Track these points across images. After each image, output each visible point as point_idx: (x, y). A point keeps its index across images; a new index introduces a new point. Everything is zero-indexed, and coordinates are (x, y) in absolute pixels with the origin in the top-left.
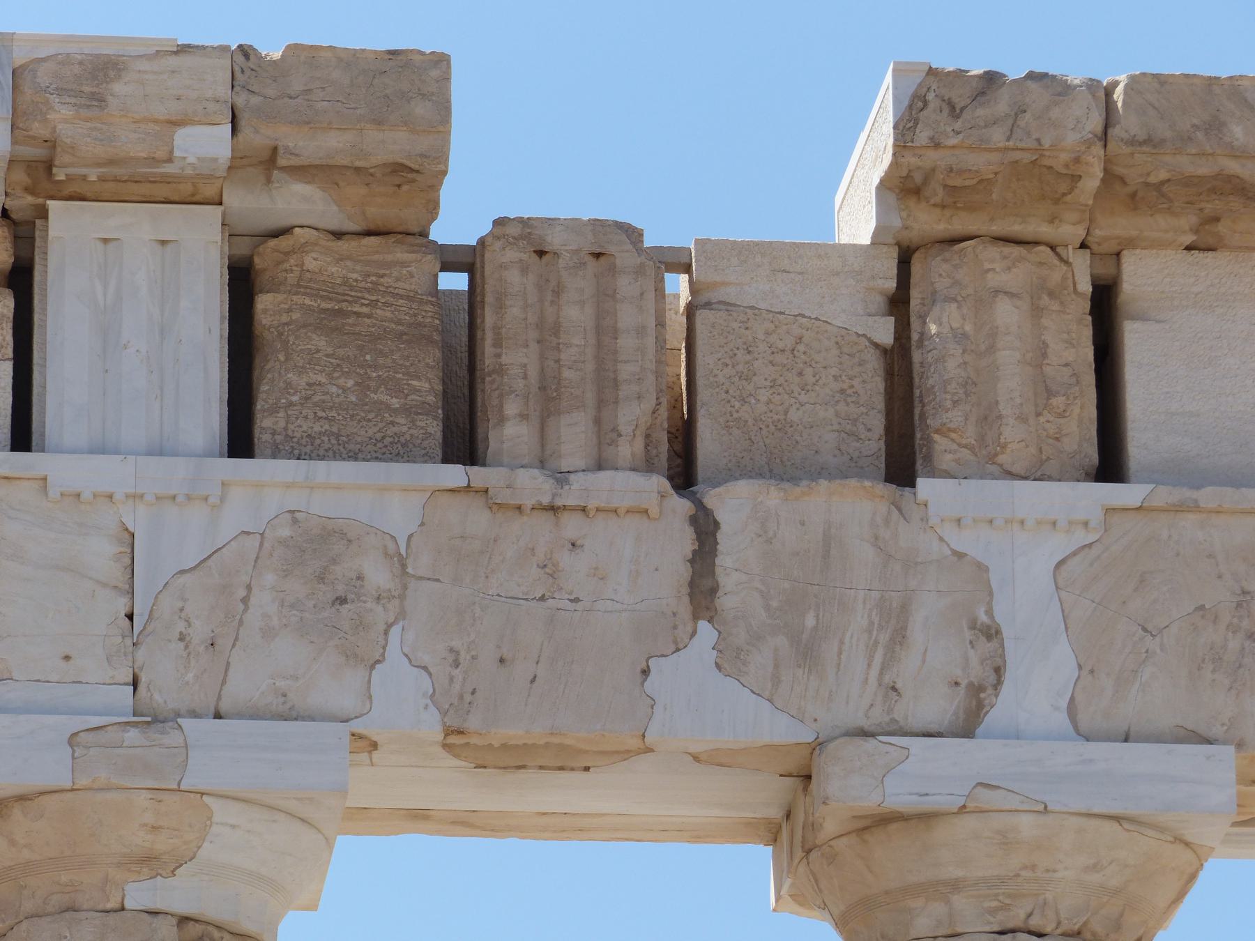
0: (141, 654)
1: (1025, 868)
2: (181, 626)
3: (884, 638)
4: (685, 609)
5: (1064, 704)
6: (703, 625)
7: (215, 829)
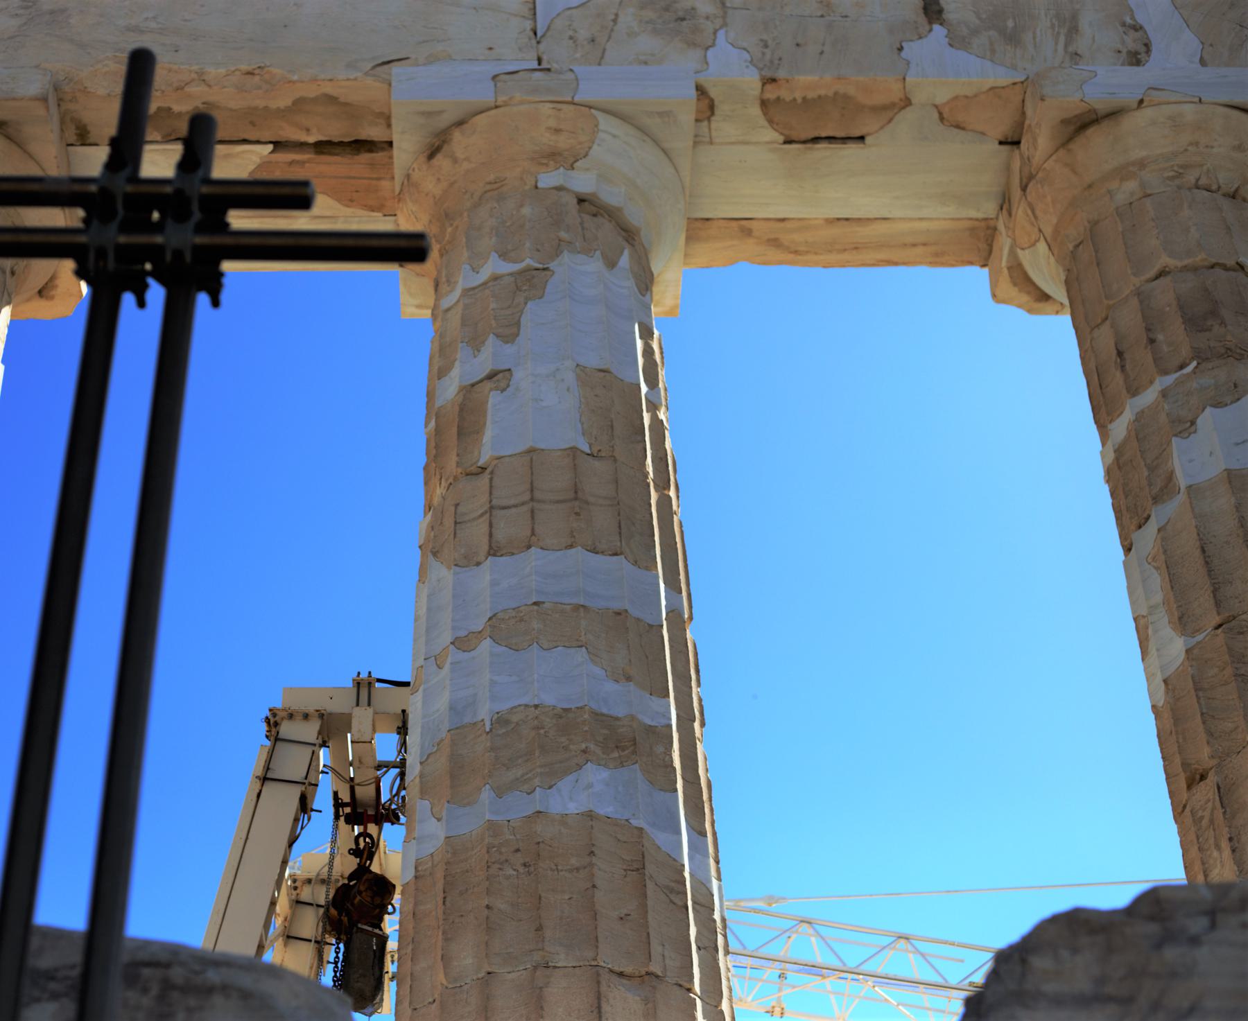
0: (542, 47)
1: (1191, 144)
2: (571, 33)
3: (1063, 31)
4: (922, 19)
5: (1197, 59)
6: (936, 27)
7: (601, 135)
